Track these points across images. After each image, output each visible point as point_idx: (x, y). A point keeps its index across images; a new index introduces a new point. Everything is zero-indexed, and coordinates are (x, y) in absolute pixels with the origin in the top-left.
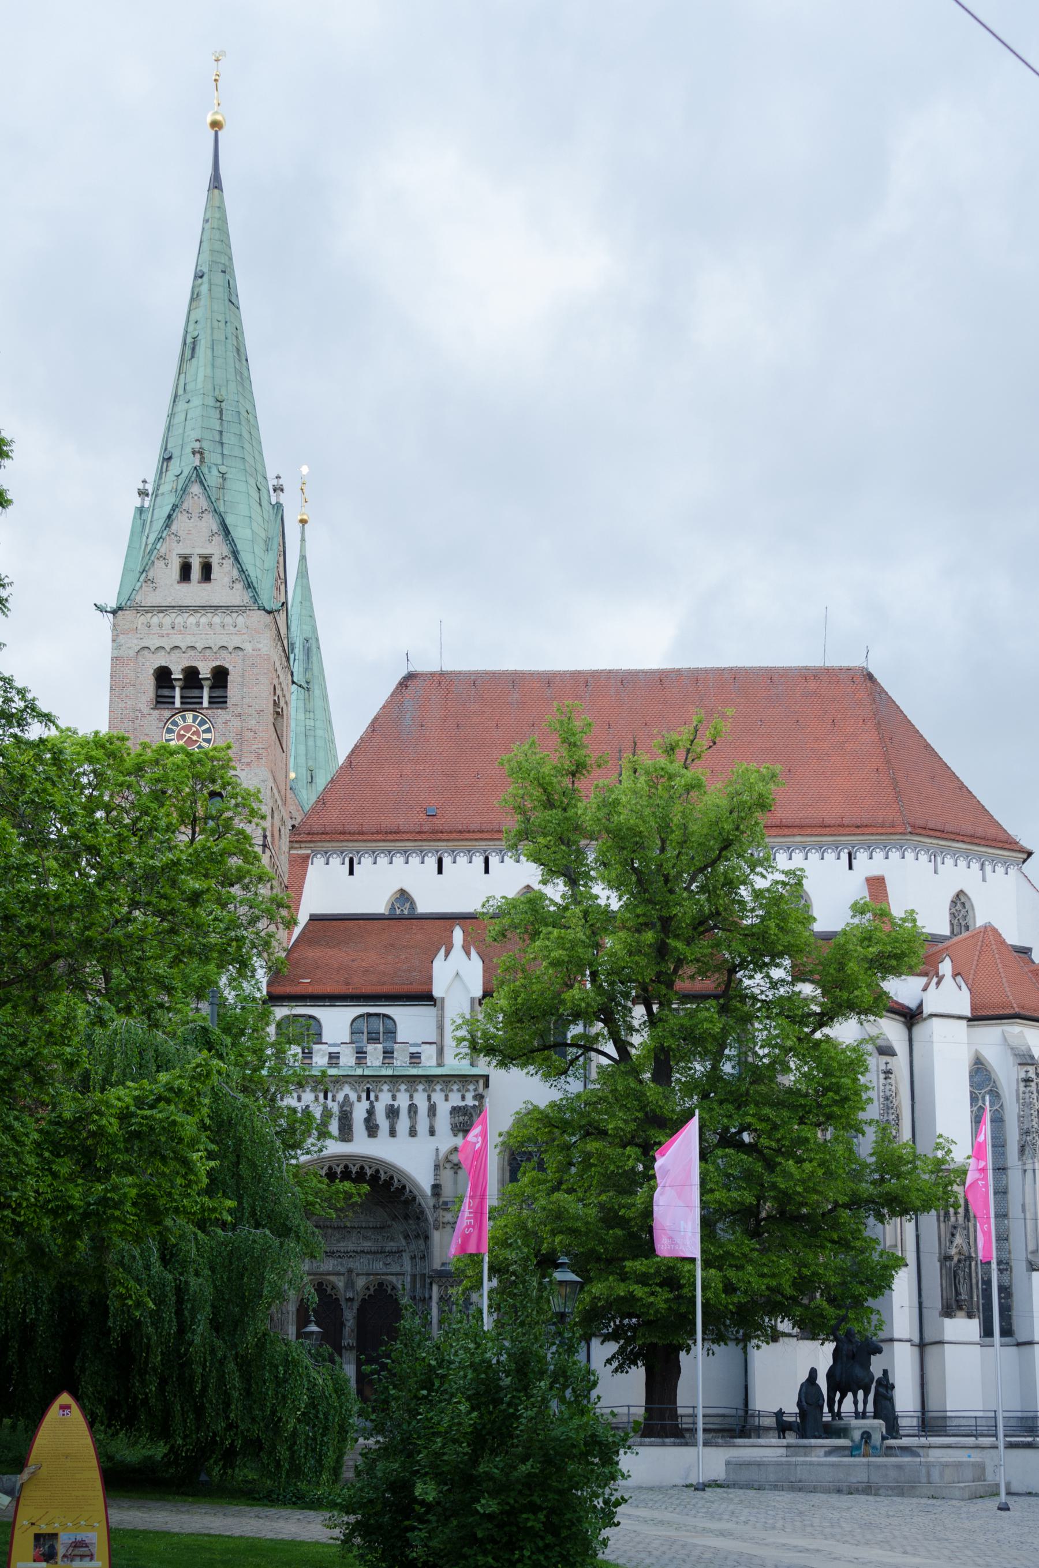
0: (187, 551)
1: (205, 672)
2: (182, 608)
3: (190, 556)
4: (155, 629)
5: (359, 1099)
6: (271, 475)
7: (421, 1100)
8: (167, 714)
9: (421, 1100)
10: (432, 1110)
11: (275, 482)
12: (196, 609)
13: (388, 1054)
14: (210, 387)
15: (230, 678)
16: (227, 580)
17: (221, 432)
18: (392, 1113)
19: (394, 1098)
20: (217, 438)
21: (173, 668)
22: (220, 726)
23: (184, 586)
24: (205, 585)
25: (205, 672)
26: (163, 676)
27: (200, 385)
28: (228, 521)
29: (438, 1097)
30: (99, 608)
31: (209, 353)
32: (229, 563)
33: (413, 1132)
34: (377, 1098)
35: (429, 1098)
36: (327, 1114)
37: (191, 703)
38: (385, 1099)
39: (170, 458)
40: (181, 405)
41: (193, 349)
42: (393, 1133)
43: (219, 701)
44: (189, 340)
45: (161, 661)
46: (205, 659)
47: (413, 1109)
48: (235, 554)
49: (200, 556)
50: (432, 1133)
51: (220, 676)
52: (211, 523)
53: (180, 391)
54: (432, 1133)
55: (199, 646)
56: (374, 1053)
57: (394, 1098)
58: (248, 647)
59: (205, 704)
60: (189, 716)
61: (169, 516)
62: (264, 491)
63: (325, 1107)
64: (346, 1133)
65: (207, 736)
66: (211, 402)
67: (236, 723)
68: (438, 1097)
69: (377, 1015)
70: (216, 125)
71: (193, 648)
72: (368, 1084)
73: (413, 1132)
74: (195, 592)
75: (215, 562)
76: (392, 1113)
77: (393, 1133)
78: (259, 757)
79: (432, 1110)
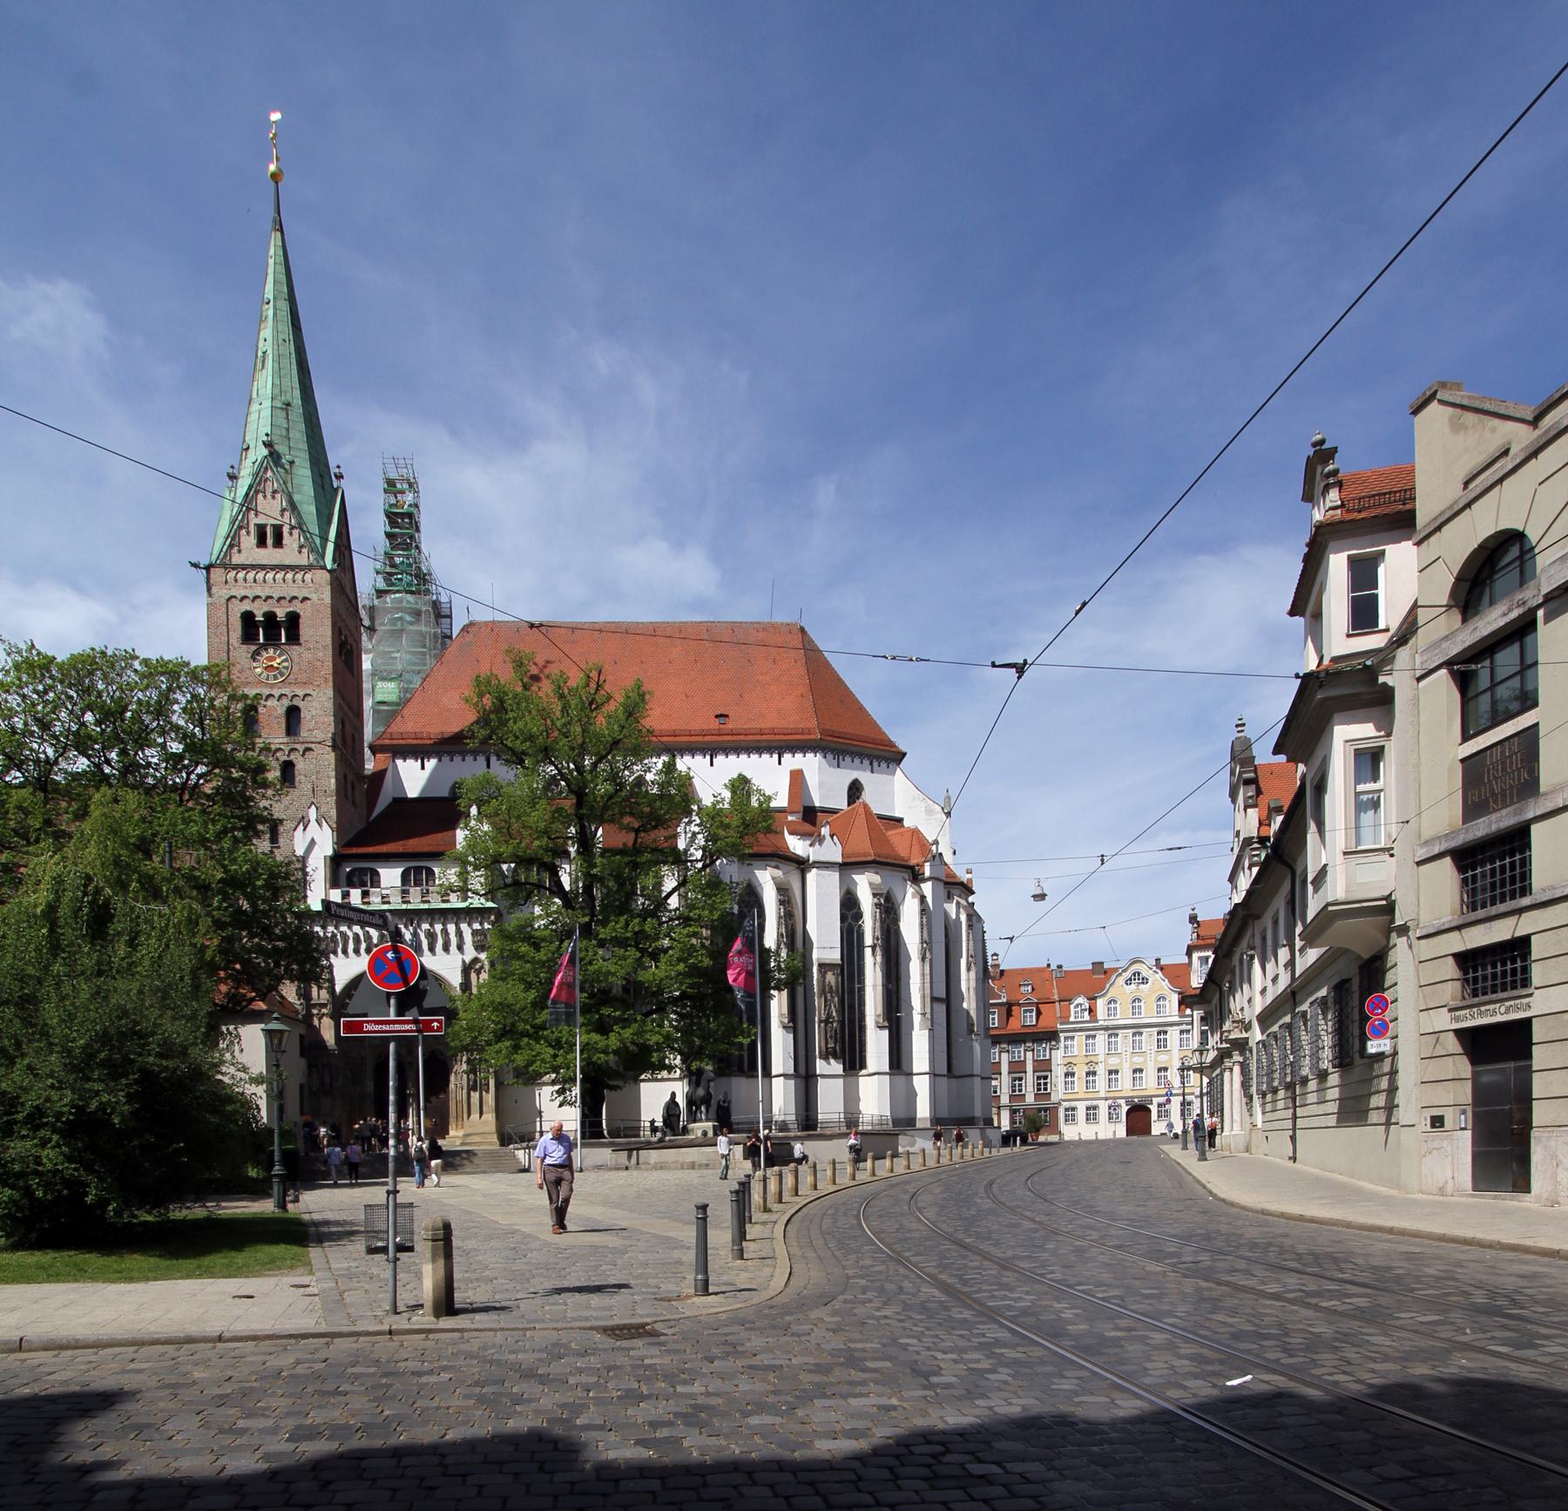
0: (263, 522)
1: (281, 614)
2: (263, 567)
3: (265, 526)
6: (332, 464)
7: (451, 928)
8: (254, 648)
9: (451, 928)
10: (459, 933)
11: (337, 470)
12: (273, 568)
13: (425, 894)
14: (277, 391)
15: (301, 621)
16: (296, 546)
17: (288, 430)
18: (431, 937)
20: (284, 433)
21: (256, 612)
22: (296, 659)
23: (262, 551)
25: (281, 614)
26: (248, 618)
27: (269, 391)
28: (296, 497)
29: (464, 927)
30: (195, 565)
31: (276, 365)
32: (296, 532)
33: (446, 948)
37: (272, 639)
38: (425, 926)
39: (248, 448)
40: (255, 407)
41: (263, 362)
43: (294, 638)
44: (260, 354)
47: (445, 932)
48: (301, 526)
49: (274, 526)
50: (460, 948)
51: (293, 619)
52: (280, 501)
53: (254, 395)
54: (460, 948)
55: (276, 596)
56: (415, 893)
58: (314, 597)
59: (283, 641)
60: (271, 651)
61: (247, 494)
62: (327, 477)
65: (285, 664)
66: (279, 405)
67: (307, 656)
68: (464, 927)
69: (422, 868)
70: (275, 177)
71: (271, 597)
73: (446, 948)
74: (269, 555)
75: (286, 530)
76: (431, 937)
77: (432, 949)
78: (326, 681)
79: (459, 933)
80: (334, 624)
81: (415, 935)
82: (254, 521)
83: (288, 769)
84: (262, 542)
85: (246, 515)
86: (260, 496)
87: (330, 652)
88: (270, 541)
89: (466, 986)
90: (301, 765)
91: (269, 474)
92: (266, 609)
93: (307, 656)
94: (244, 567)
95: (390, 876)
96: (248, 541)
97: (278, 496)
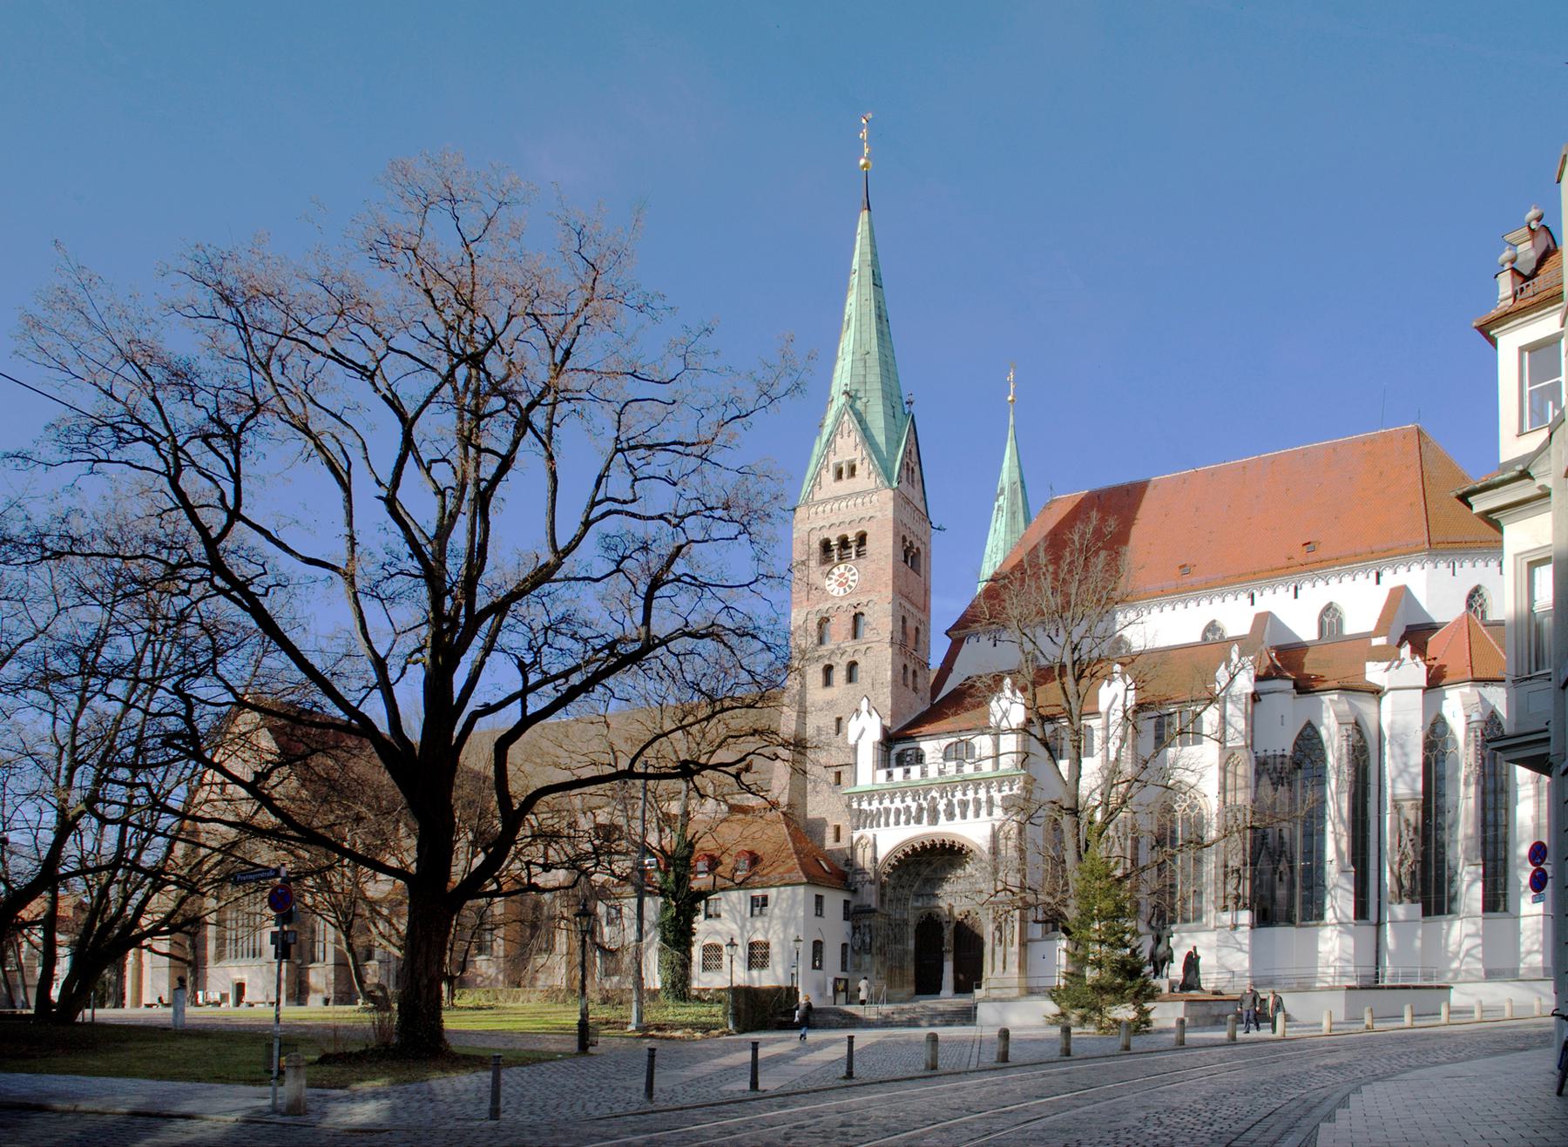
1: (852, 537)
2: (837, 498)
4: (821, 515)
5: (942, 797)
8: (828, 568)
9: (982, 794)
16: (866, 474)
19: (965, 794)
23: (839, 484)
24: (852, 480)
25: (852, 537)
26: (826, 546)
32: (866, 462)
34: (953, 796)
35: (988, 792)
36: (920, 809)
38: (959, 795)
42: (964, 816)
45: (826, 534)
46: (852, 528)
50: (990, 814)
51: (862, 539)
54: (990, 814)
55: (847, 520)
57: (965, 794)
58: (879, 515)
60: (842, 567)
63: (920, 806)
64: (934, 820)
67: (873, 566)
72: (946, 787)
73: (977, 815)
74: (846, 485)
80: (896, 534)
81: (950, 805)
82: (834, 460)
83: (852, 666)
84: (839, 475)
85: (827, 457)
86: (838, 437)
87: (891, 560)
88: (845, 475)
89: (995, 850)
90: (863, 664)
91: (846, 417)
92: (839, 533)
93: (873, 566)
94: (824, 502)
95: (931, 748)
96: (828, 476)
97: (853, 434)
